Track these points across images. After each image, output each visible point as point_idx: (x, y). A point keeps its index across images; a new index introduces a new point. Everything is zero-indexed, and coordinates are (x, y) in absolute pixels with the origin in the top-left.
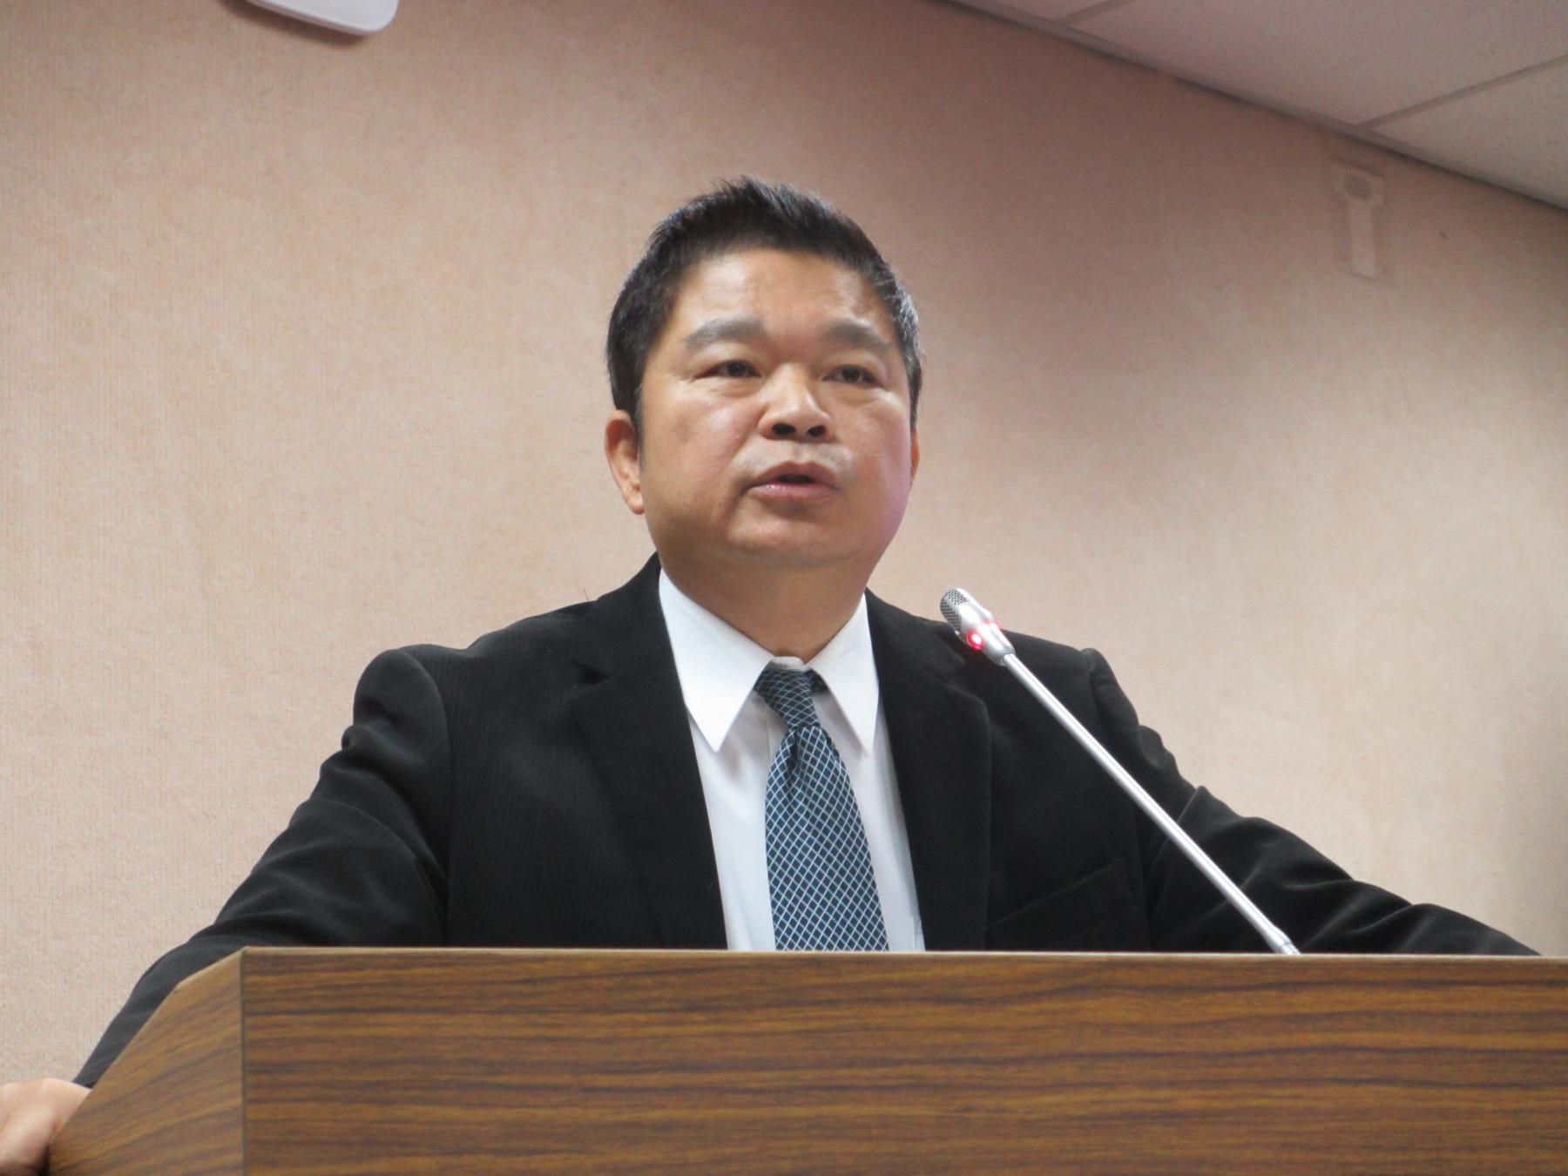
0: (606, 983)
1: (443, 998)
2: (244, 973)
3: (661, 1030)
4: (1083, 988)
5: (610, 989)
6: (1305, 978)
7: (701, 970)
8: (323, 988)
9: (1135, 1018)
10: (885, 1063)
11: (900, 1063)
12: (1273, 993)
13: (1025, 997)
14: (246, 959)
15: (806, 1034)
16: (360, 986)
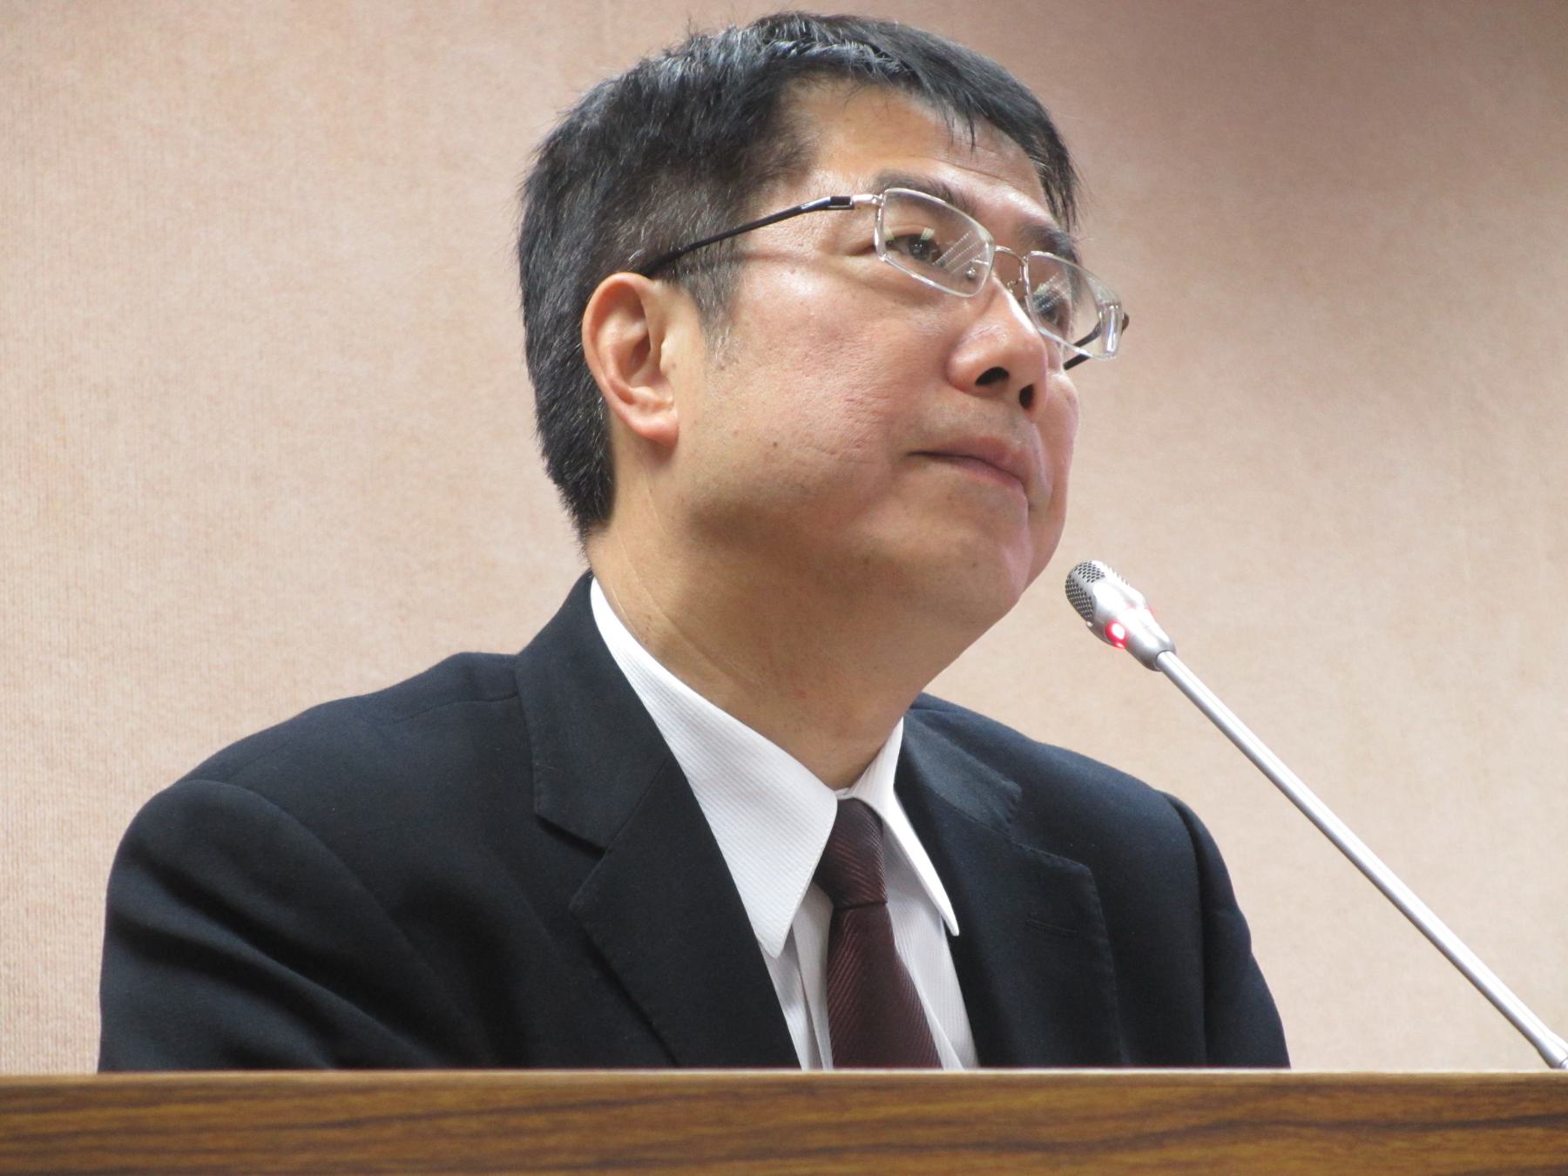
0: (475, 1124)
1: (209, 1151)
8: (16, 1139)
12: (1537, 1132)
13: (1134, 1143)
16: (76, 1134)
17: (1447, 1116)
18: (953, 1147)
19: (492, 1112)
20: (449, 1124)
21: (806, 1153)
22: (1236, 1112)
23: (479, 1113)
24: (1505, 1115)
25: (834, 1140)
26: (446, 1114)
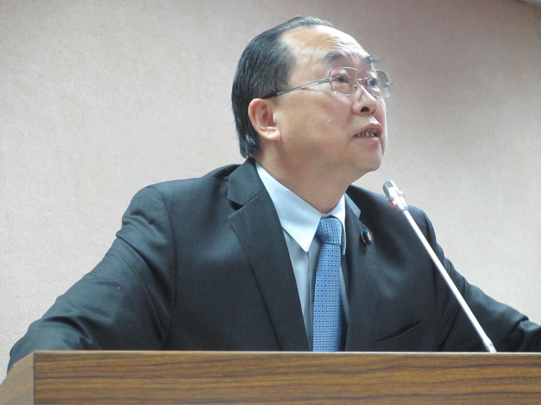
0: (190, 365)
1: (119, 372)
2: (35, 361)
4: (394, 367)
5: (191, 368)
6: (489, 363)
7: (230, 360)
8: (69, 368)
9: (416, 380)
11: (315, 399)
12: (475, 369)
13: (367, 372)
14: (36, 355)
15: (274, 387)
17: (451, 365)
18: (318, 372)
19: (194, 362)
20: (183, 365)
21: (279, 374)
22: (395, 364)
23: (191, 362)
24: (467, 365)
25: (286, 370)
26: (182, 363)
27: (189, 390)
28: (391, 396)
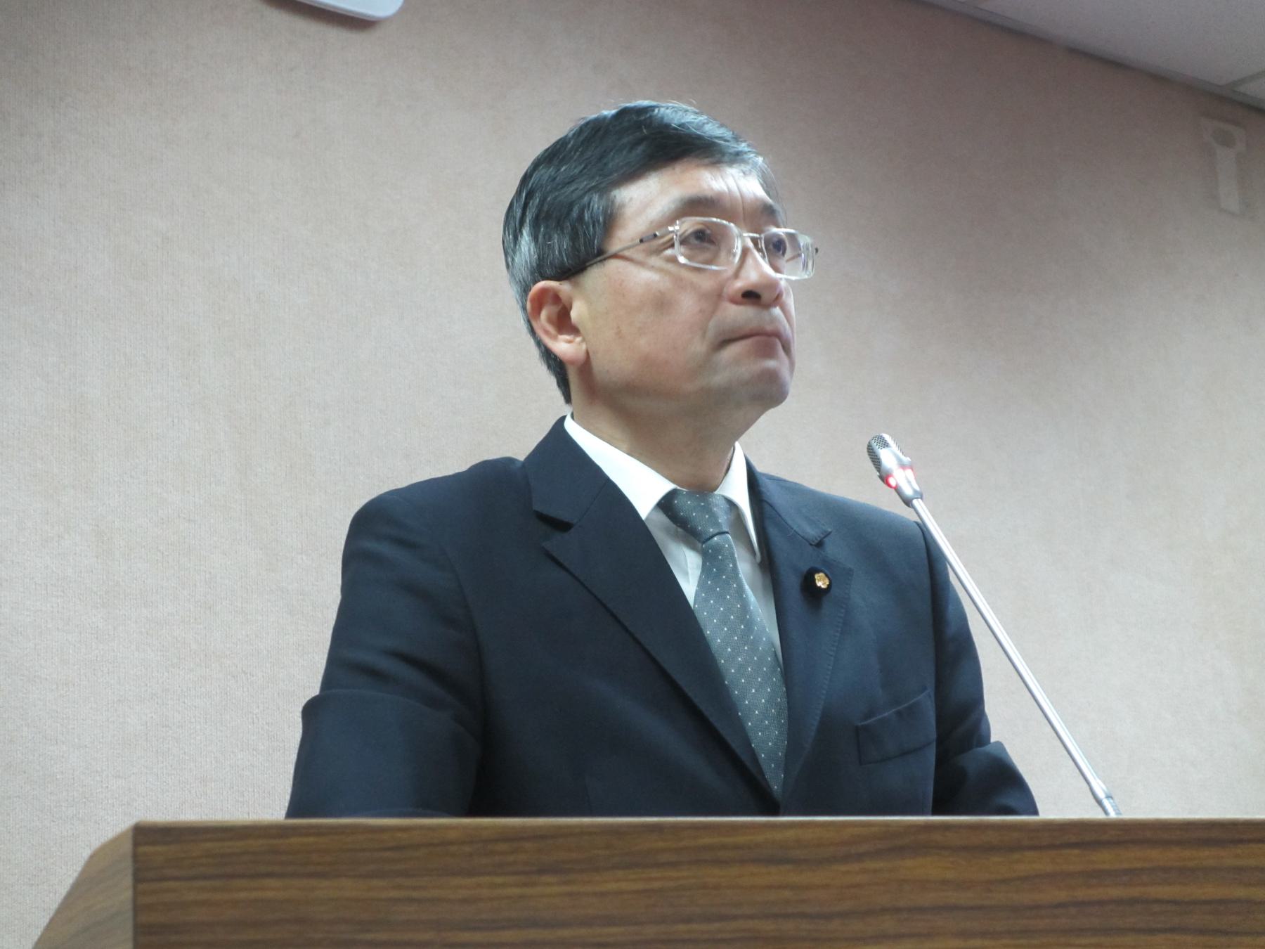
0: (467, 849)
2: (136, 844)
3: (516, 891)
9: (950, 875)
10: (722, 918)
11: (735, 918)
12: (1076, 851)
13: (846, 858)
21: (659, 865)
26: (451, 843)
27: (464, 901)
28: (897, 910)
